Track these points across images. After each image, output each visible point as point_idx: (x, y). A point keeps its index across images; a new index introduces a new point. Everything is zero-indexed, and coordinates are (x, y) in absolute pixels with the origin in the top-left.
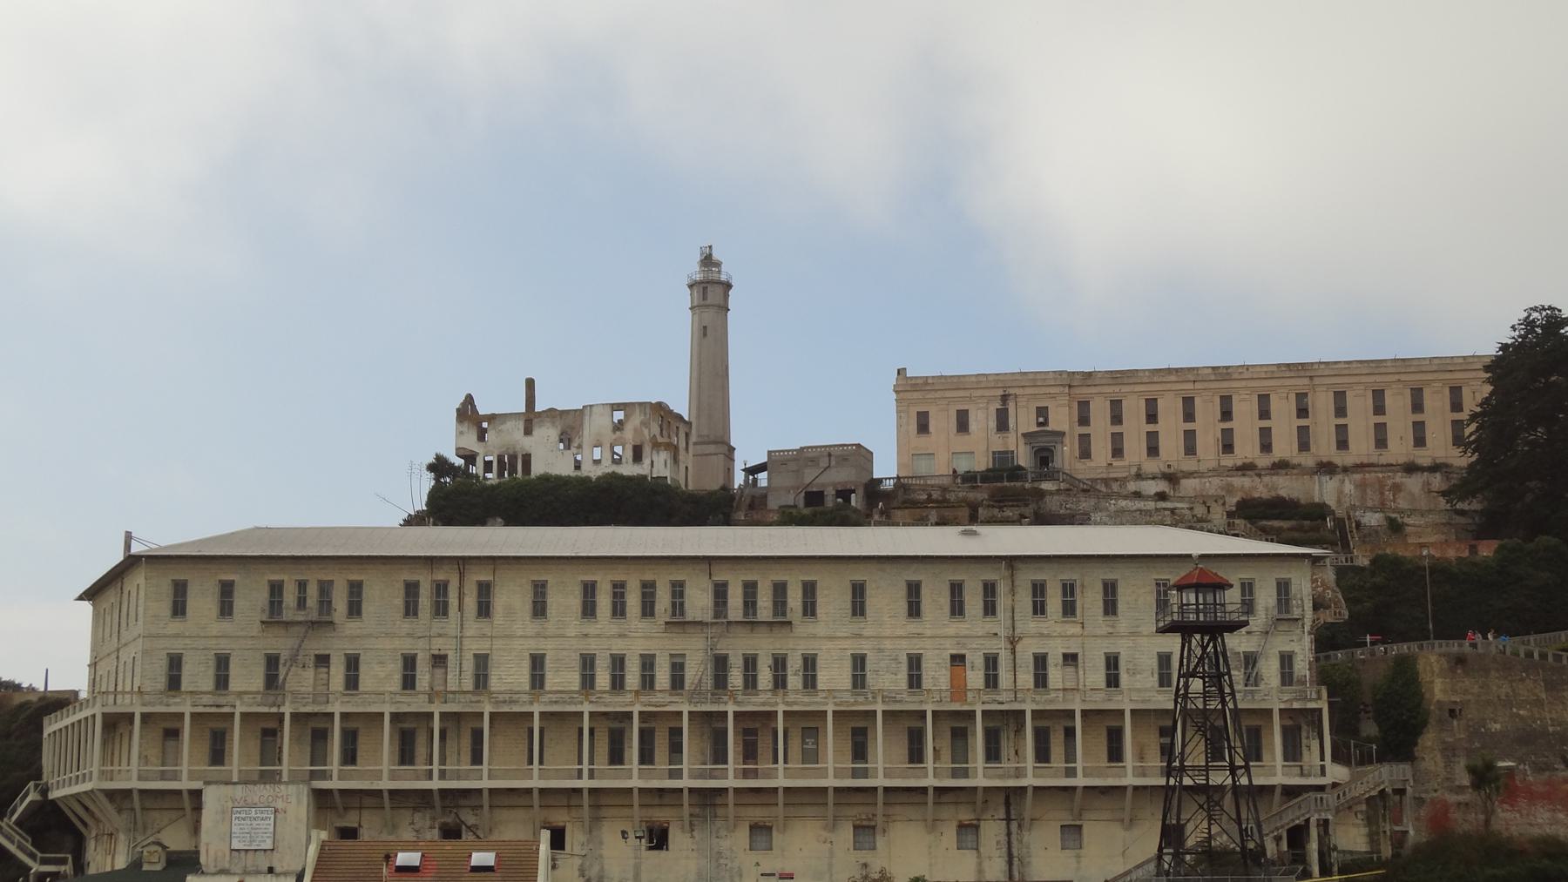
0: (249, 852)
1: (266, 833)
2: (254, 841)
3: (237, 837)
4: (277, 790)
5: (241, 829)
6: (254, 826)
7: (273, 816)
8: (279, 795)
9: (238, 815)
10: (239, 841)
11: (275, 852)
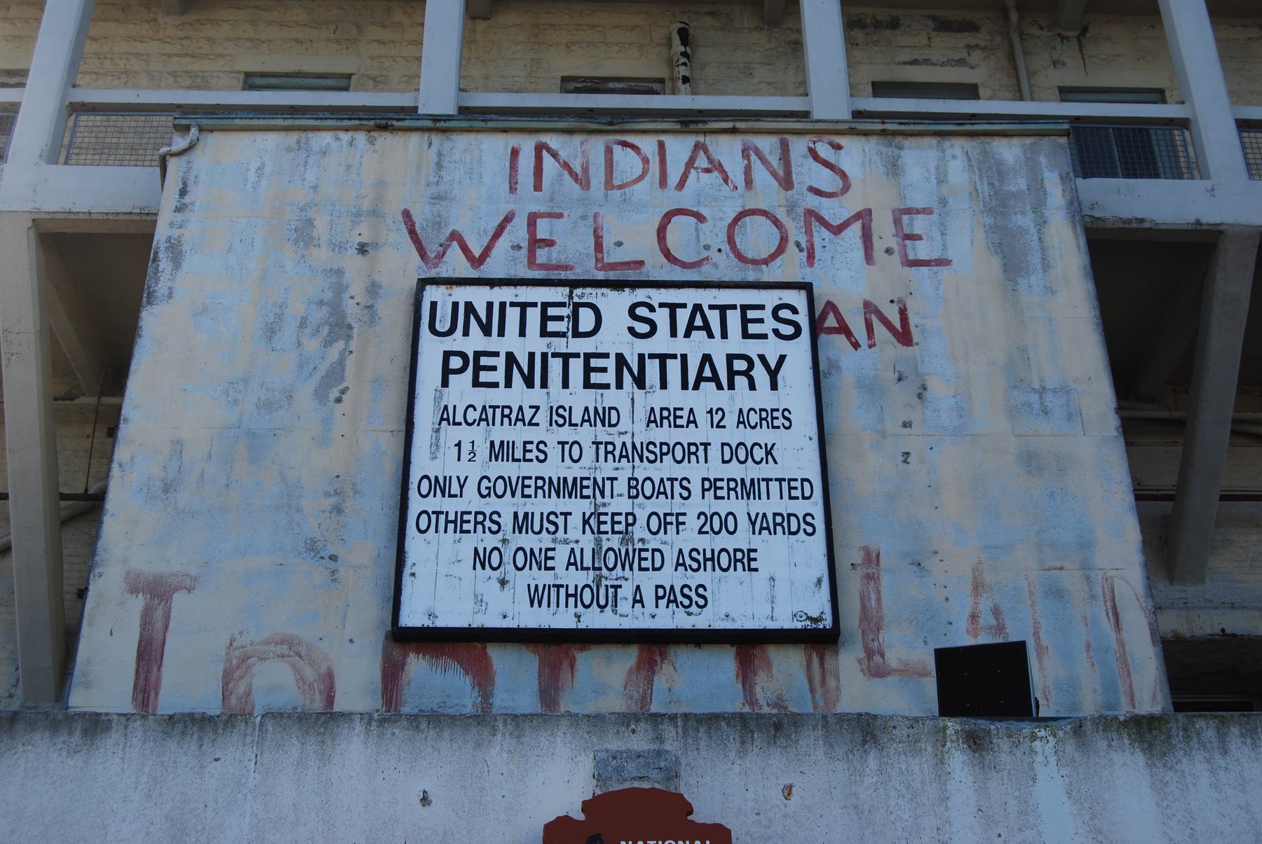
0: (589, 663)
1: (749, 489)
2: (631, 558)
3: (459, 523)
4: (809, 173)
5: (500, 451)
6: (634, 429)
7: (798, 352)
8: (834, 211)
9: (475, 341)
10: (481, 559)
11: (848, 661)
